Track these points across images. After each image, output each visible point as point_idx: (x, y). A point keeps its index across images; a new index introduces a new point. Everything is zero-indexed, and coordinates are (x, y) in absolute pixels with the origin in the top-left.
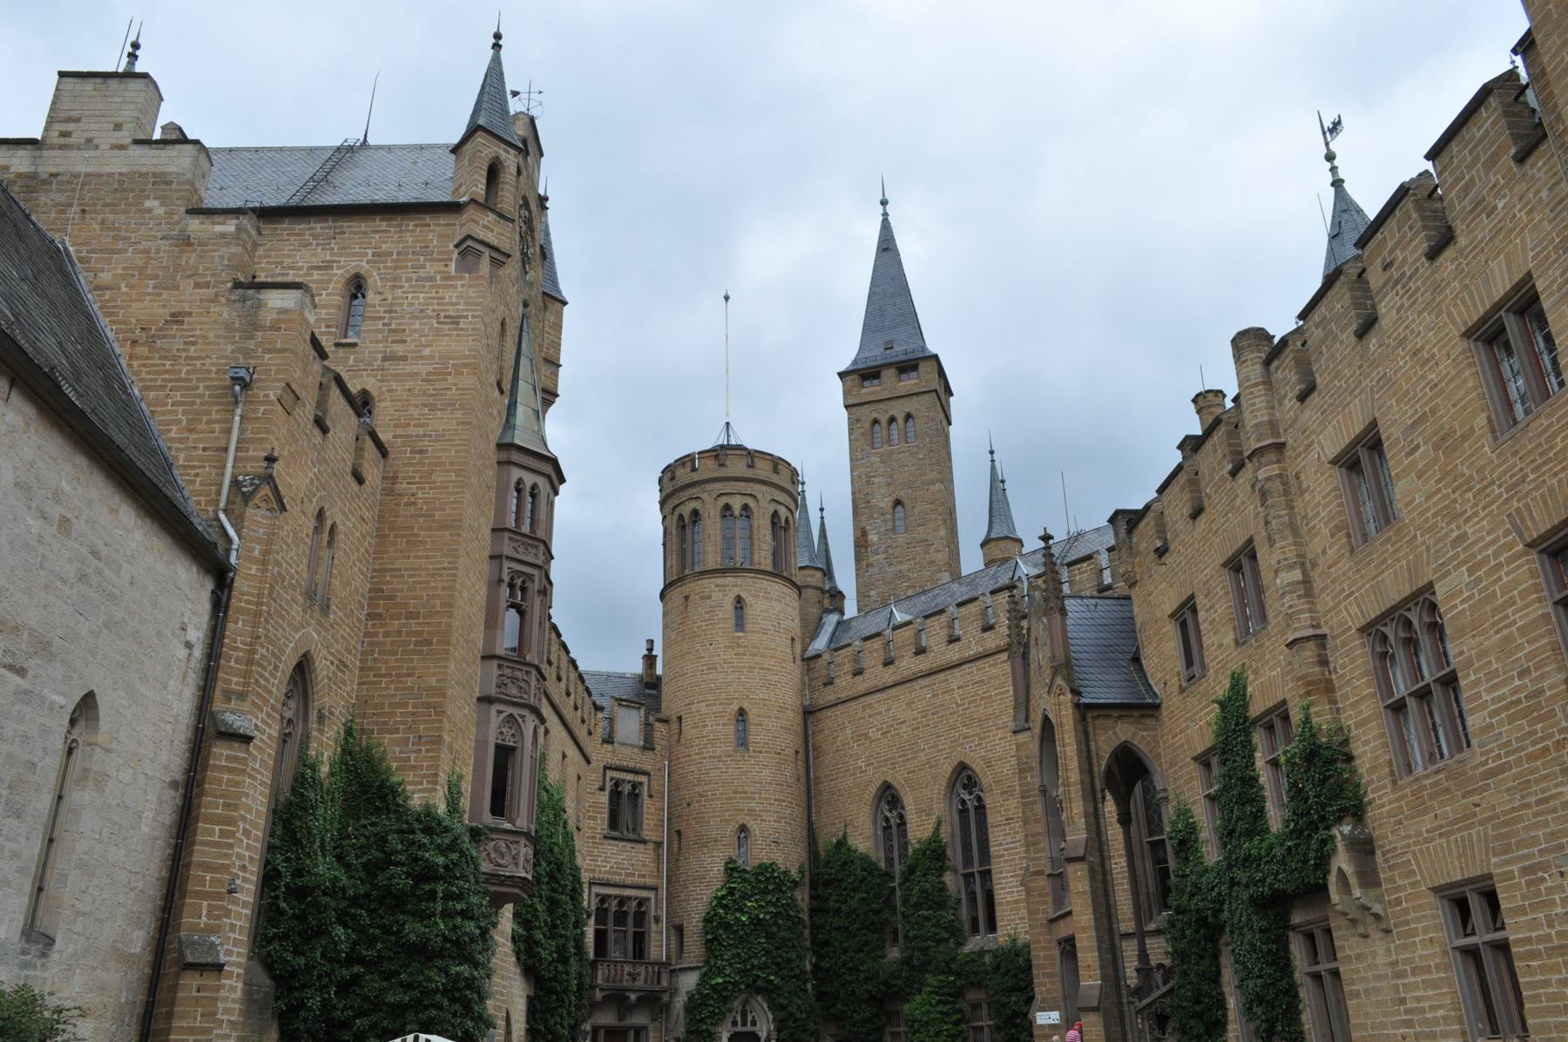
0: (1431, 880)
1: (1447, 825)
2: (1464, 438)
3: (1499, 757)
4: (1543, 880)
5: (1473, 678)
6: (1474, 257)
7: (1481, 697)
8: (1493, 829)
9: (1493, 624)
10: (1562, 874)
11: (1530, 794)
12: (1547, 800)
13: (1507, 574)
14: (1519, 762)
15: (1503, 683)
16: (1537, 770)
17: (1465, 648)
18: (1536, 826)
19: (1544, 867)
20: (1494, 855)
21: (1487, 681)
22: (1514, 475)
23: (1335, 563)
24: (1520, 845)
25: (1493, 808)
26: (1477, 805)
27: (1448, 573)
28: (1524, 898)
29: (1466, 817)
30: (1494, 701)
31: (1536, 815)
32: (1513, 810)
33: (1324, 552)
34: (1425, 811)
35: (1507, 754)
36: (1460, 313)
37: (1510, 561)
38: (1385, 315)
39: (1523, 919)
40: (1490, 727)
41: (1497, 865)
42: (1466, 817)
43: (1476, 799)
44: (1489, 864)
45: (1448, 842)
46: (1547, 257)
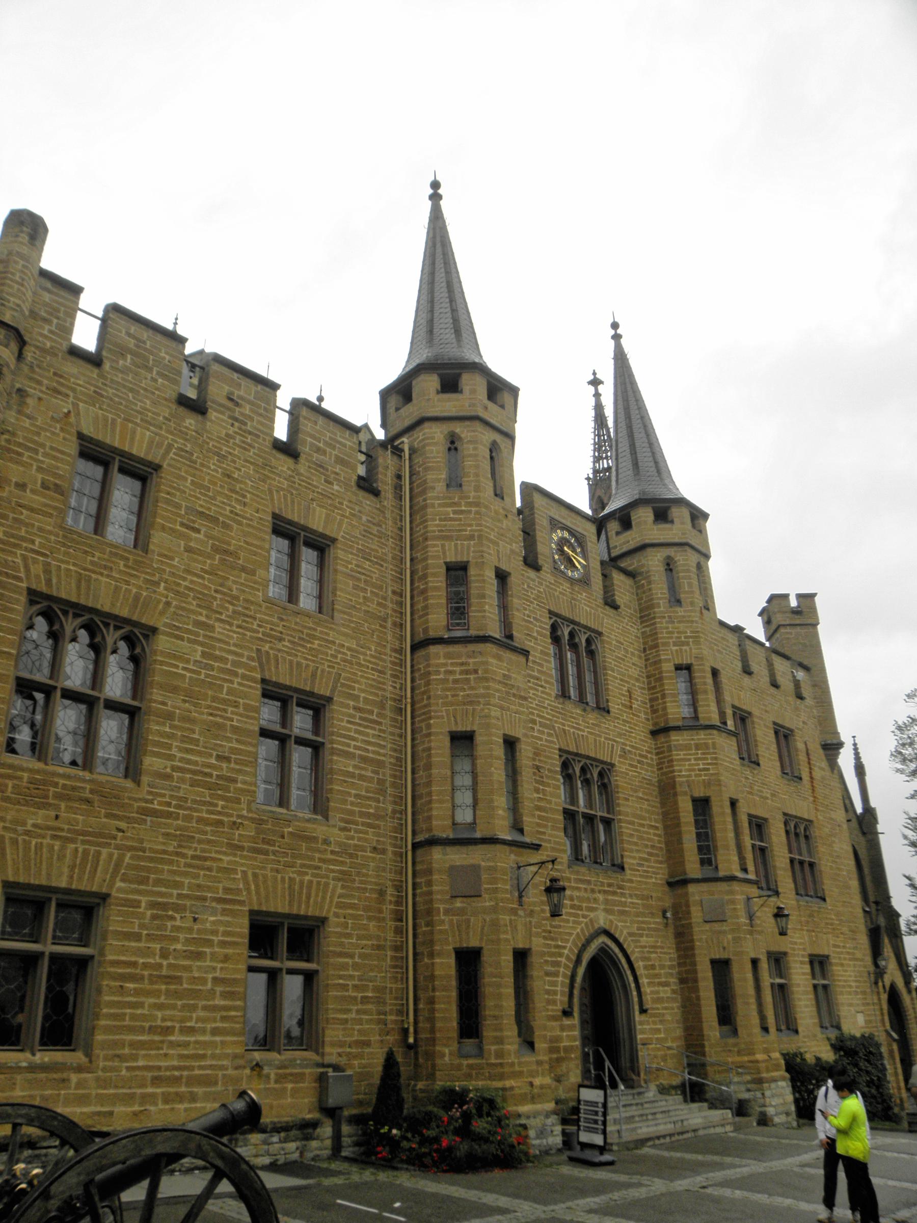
0: (16, 872)
1: (69, 831)
2: (243, 569)
3: (169, 804)
4: (172, 918)
5: (167, 729)
6: (306, 488)
7: (170, 749)
8: (131, 858)
9: (209, 707)
10: (195, 920)
11: (190, 848)
12: (206, 859)
13: (239, 684)
14: (188, 818)
15: (200, 753)
16: (205, 833)
17: (170, 703)
18: (185, 874)
19: (178, 908)
20: (123, 880)
21: (182, 741)
22: (275, 631)
23: (32, 510)
24: (158, 882)
25: (141, 841)
26: (119, 830)
27: (182, 639)
28: (142, 926)
29: (101, 835)
30: (182, 760)
31: (186, 865)
32: (164, 852)
33: (22, 486)
34: (45, 806)
35: (179, 807)
36: (279, 499)
37: (244, 677)
38: (211, 421)
39: (133, 944)
40: (168, 777)
41: (119, 890)
42: (101, 835)
43: (123, 825)
44: (112, 885)
45: (63, 848)
46: (351, 547)
